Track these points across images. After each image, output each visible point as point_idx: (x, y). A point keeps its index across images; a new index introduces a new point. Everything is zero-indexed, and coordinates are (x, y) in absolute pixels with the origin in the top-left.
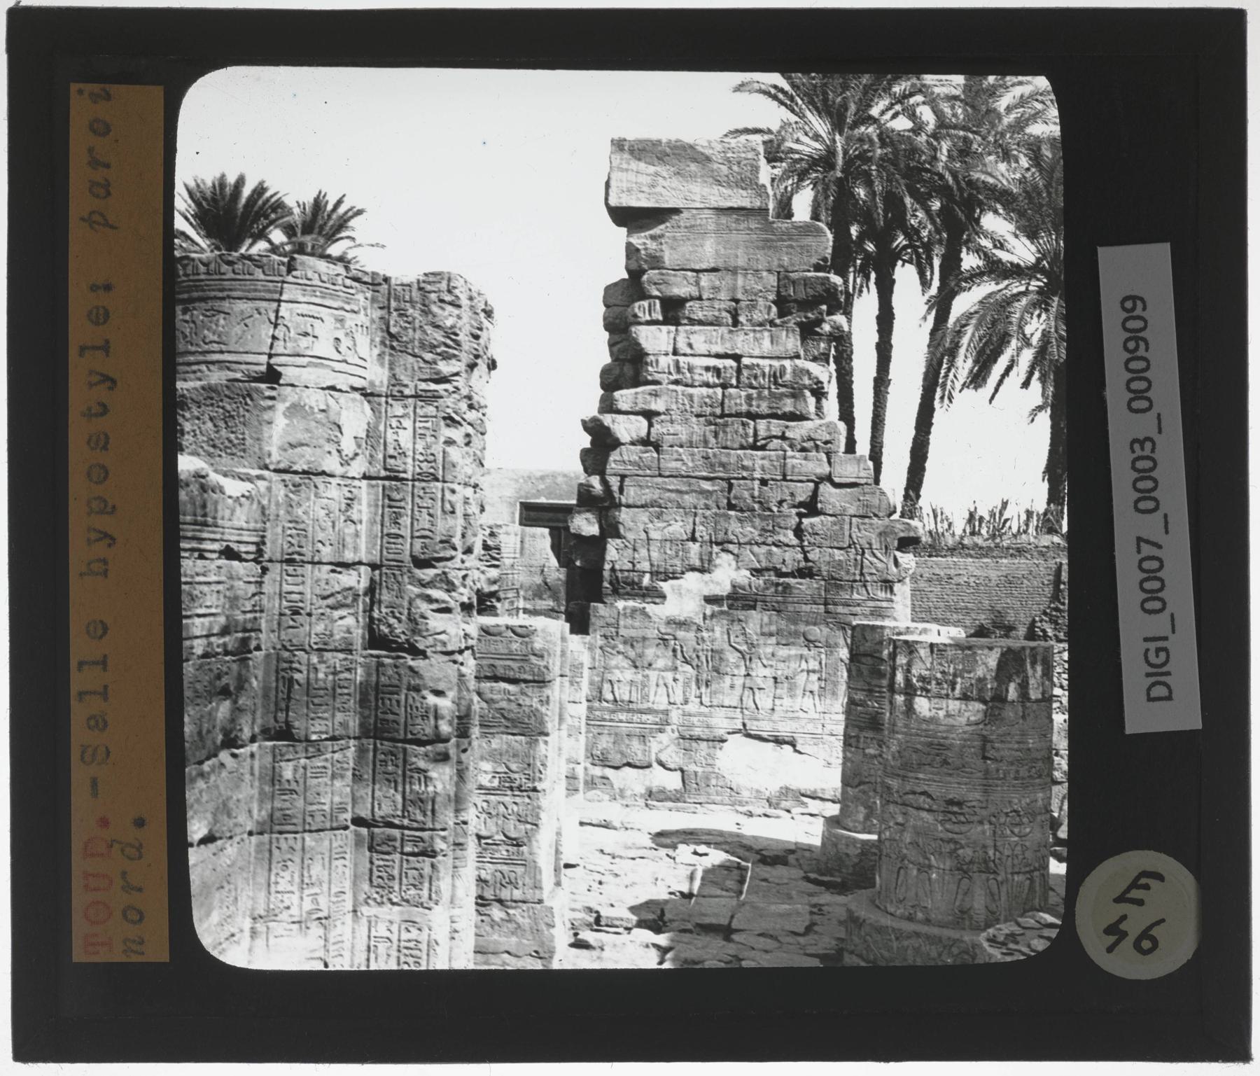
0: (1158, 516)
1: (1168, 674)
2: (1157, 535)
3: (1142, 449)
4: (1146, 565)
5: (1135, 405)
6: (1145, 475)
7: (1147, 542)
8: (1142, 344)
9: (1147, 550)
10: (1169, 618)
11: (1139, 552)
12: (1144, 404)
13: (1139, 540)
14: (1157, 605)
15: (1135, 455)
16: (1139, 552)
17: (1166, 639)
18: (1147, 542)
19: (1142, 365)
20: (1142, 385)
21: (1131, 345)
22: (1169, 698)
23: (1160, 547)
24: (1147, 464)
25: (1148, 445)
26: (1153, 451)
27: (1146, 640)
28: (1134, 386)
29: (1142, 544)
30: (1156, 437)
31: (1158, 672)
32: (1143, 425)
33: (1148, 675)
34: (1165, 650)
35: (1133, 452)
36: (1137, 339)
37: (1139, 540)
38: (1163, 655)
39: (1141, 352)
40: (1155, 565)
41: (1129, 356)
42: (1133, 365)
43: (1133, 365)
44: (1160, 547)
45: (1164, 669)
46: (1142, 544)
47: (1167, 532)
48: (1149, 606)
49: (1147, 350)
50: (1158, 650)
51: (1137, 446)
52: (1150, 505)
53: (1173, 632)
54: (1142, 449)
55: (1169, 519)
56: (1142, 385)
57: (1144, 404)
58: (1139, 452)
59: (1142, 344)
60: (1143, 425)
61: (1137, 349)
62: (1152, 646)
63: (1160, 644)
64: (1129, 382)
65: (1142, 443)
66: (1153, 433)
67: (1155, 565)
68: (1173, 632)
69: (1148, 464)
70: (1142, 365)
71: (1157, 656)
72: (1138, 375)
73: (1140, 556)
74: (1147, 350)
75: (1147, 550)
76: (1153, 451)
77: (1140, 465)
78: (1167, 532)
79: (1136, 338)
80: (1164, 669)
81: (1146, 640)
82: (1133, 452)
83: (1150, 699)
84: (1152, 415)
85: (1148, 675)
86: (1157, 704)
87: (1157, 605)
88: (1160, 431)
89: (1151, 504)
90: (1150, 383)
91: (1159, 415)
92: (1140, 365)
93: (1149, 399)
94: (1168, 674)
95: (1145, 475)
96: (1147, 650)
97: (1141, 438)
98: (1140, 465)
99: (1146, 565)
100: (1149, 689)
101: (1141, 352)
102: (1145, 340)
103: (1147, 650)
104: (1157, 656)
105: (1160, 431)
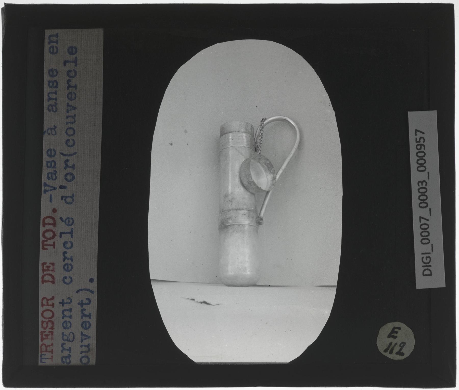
3: (422, 185)
6: (423, 194)
15: (420, 187)
24: (424, 190)
25: (424, 184)
26: (426, 185)
28: (420, 162)
30: (427, 180)
32: (422, 176)
35: (419, 186)
48: (422, 205)
51: (420, 184)
54: (422, 185)
55: (431, 210)
58: (421, 186)
60: (422, 176)
64: (418, 160)
65: (422, 183)
66: (426, 179)
69: (424, 190)
76: (426, 185)
82: (419, 186)
84: (426, 173)
95: (423, 194)
97: (422, 181)
98: (421, 190)
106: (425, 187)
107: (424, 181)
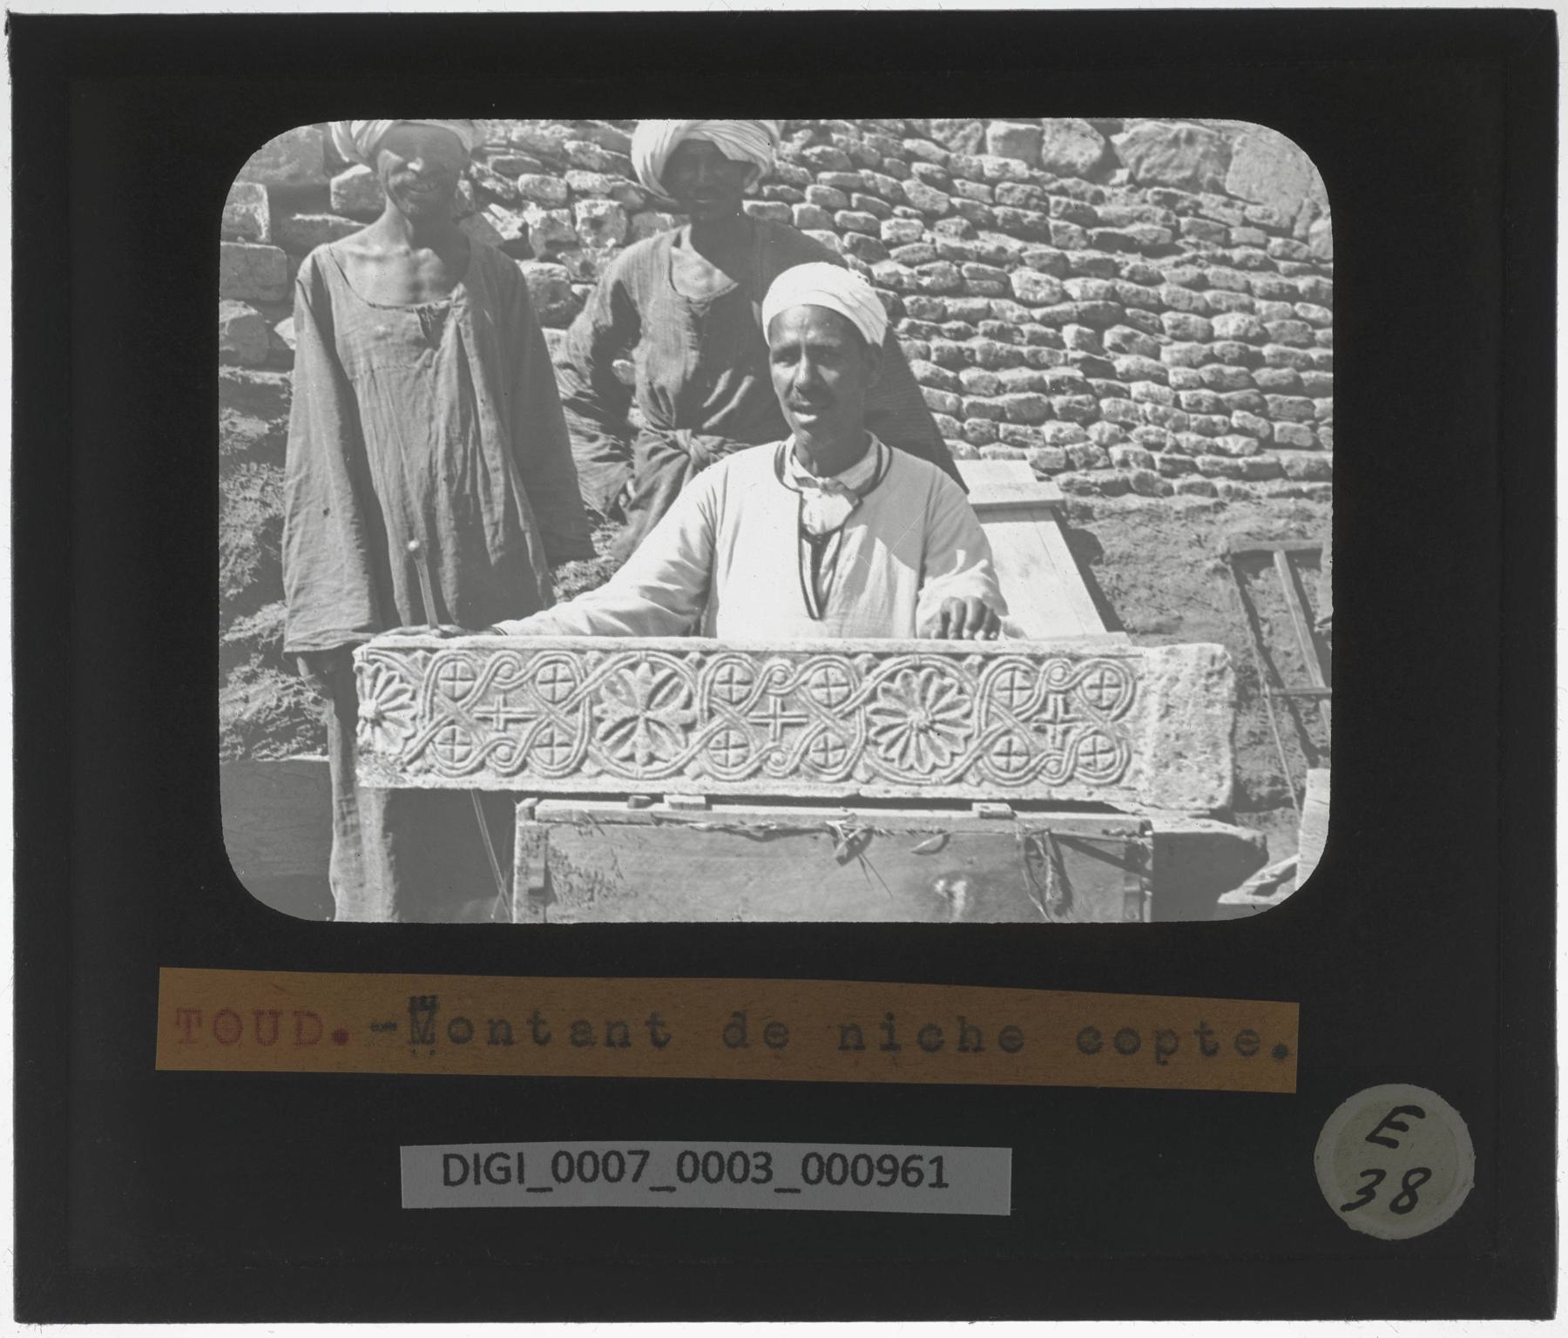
0: (673, 1180)
1: (477, 1182)
2: (651, 1176)
3: (757, 1167)
4: (613, 1161)
5: (813, 1163)
7: (641, 1166)
8: (888, 1178)
9: (632, 1163)
10: (545, 1185)
11: (631, 1153)
12: (813, 1174)
13: (646, 1154)
14: (563, 1172)
15: (750, 1157)
16: (631, 1153)
17: (521, 1180)
18: (641, 1166)
19: (862, 1176)
20: (837, 1172)
21: (888, 1164)
22: (447, 1182)
23: (636, 1178)
24: (738, 1173)
25: (761, 1174)
26: (756, 1181)
27: (520, 1156)
29: (638, 1158)
30: (772, 1185)
31: (479, 1171)
33: (477, 1157)
34: (507, 1179)
35: (756, 1155)
36: (894, 1172)
37: (646, 1154)
38: (500, 1175)
39: (878, 1176)
40: (614, 1171)
41: (875, 1163)
42: (863, 1164)
43: (863, 1167)
44: (636, 1178)
45: (483, 1176)
46: (638, 1158)
47: (652, 1189)
49: (880, 1183)
50: (507, 1170)
51: (761, 1160)
52: (688, 1172)
53: (529, 1190)
54: (757, 1167)
56: (837, 1172)
57: (813, 1174)
58: (753, 1162)
59: (888, 1178)
61: (881, 1169)
62: (513, 1164)
63: (514, 1173)
65: (765, 1167)
66: (778, 1180)
67: (614, 1171)
68: (529, 1190)
69: (738, 1173)
70: (862, 1176)
71: (500, 1169)
72: (850, 1170)
73: (625, 1155)
74: (880, 1183)
75: (632, 1163)
76: (756, 1181)
77: (739, 1161)
78: (652, 1189)
79: (903, 1172)
80: (483, 1176)
81: (520, 1156)
82: (756, 1155)
83: (447, 1158)
84: (799, 1183)
85: (477, 1157)
86: (441, 1170)
87: (563, 1172)
88: (778, 1190)
89: (688, 1172)
90: (840, 1182)
91: (797, 1191)
92: (862, 1173)
93: (818, 1180)
94: (477, 1182)
95: (726, 1167)
96: (507, 1157)
98: (739, 1161)
99: (613, 1161)
100: (460, 1158)
101: (878, 1176)
102: (892, 1181)
103: (507, 1157)
104: (500, 1169)
105: (778, 1190)
106: (750, 1176)
107: (769, 1177)
